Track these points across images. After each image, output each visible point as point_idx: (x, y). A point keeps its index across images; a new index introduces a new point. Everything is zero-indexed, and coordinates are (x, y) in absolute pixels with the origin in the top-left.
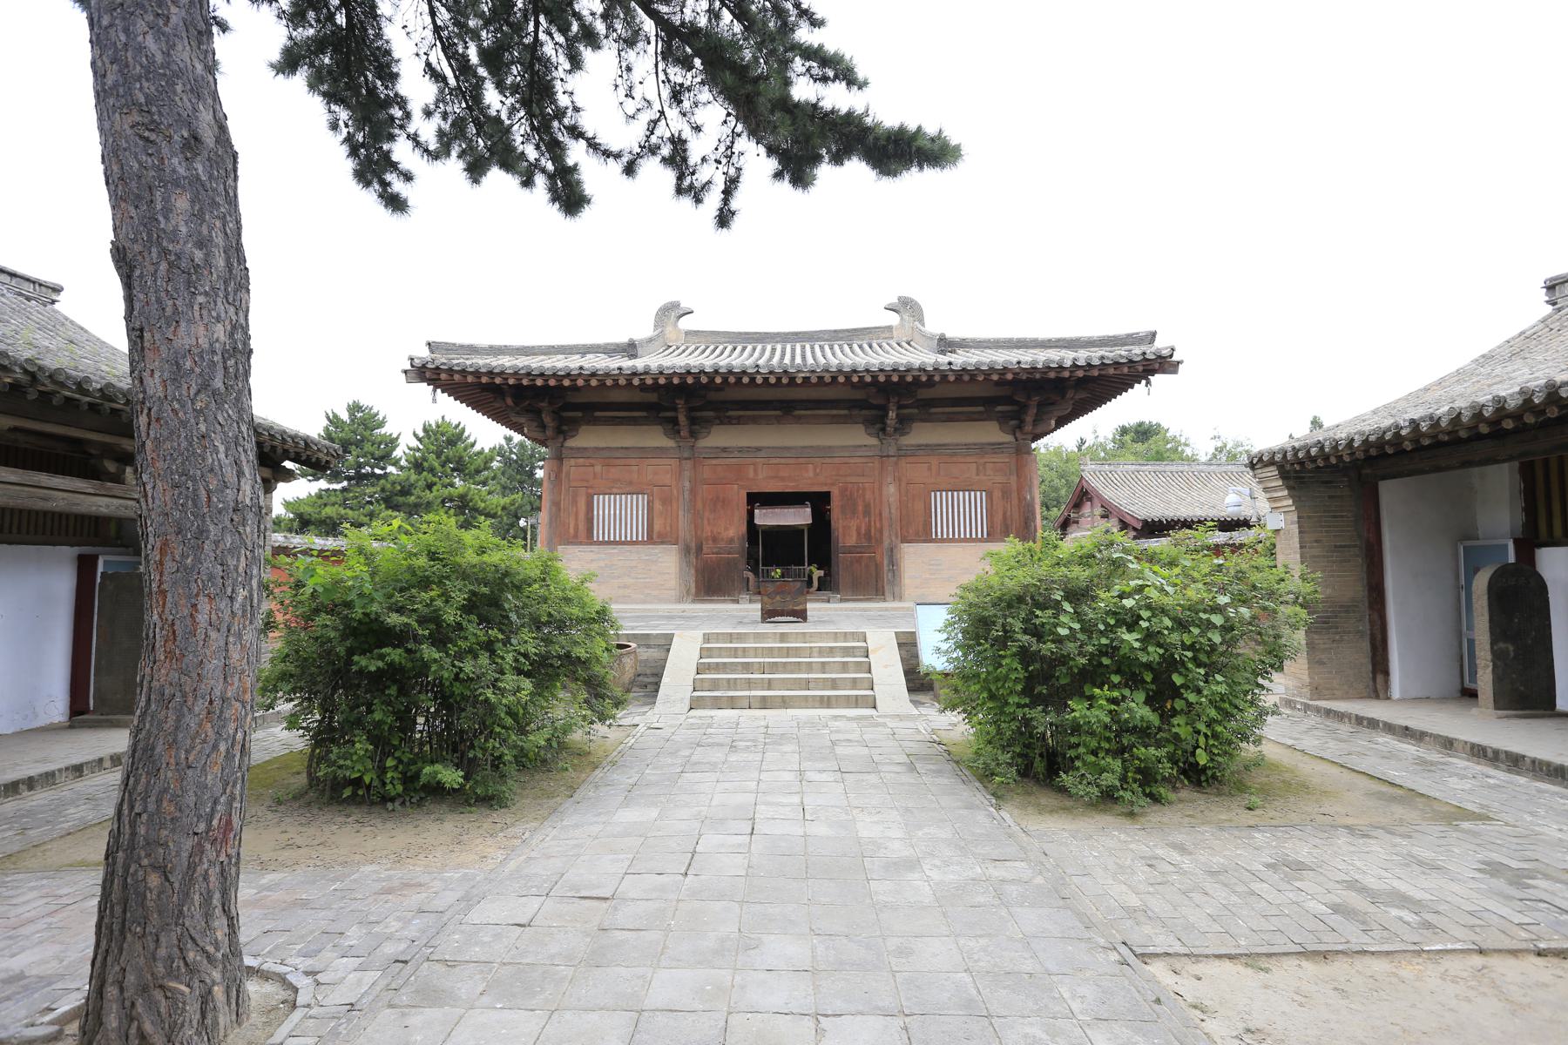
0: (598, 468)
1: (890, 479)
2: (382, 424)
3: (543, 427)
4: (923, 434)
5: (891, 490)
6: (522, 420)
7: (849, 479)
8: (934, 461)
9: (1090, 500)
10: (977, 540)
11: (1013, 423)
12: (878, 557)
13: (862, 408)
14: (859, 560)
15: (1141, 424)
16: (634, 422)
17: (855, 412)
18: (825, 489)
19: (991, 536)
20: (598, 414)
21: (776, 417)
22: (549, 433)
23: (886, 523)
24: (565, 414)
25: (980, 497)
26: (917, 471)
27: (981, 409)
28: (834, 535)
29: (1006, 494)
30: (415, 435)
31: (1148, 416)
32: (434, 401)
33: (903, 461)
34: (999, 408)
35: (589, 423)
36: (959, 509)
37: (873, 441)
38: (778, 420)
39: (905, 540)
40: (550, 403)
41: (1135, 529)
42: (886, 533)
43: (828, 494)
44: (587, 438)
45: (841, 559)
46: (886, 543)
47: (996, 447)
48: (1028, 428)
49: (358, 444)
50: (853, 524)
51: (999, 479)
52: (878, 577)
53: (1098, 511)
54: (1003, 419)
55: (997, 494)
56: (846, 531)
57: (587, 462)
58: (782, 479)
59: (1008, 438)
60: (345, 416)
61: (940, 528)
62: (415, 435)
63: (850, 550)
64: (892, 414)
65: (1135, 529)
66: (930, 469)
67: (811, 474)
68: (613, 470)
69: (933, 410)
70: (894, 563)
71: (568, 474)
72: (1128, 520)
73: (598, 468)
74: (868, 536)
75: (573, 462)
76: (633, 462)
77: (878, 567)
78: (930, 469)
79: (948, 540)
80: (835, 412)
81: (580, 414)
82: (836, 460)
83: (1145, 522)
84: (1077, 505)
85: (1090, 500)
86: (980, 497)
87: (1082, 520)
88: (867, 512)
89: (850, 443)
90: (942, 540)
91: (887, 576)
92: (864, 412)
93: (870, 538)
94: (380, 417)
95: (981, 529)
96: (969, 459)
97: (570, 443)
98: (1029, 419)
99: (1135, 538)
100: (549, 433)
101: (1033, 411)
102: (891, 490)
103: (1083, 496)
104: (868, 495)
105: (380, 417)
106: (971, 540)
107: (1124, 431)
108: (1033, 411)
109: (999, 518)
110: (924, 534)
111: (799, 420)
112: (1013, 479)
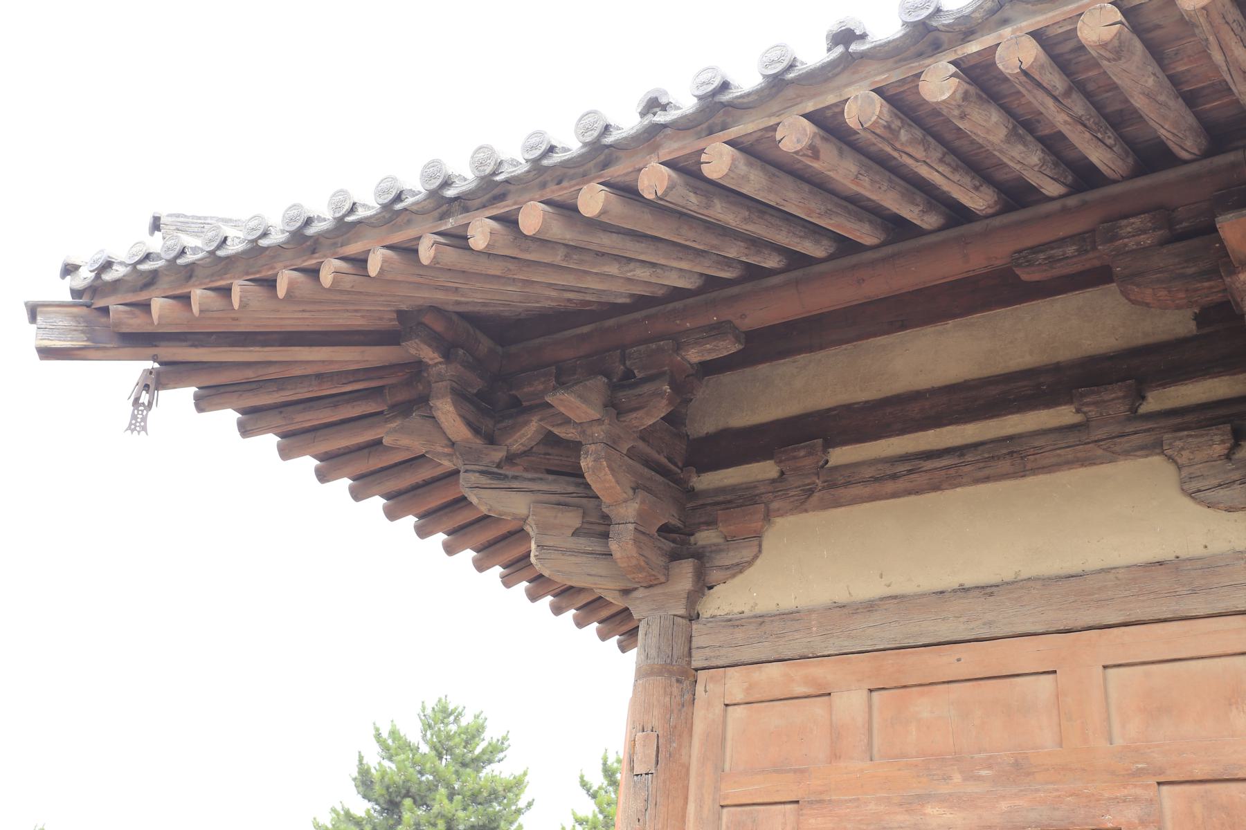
0: (850, 702)
2: (494, 752)
3: (599, 527)
6: (513, 504)
16: (1015, 459)
20: (841, 455)
22: (623, 545)
24: (708, 481)
30: (584, 784)
32: (138, 424)
35: (805, 500)
40: (615, 408)
44: (804, 566)
49: (421, 800)
57: (795, 677)
60: (413, 733)
62: (584, 784)
68: (924, 706)
71: (718, 741)
73: (850, 702)
75: (735, 683)
76: (1025, 654)
81: (765, 470)
94: (491, 734)
97: (727, 599)
100: (623, 545)
105: (491, 734)
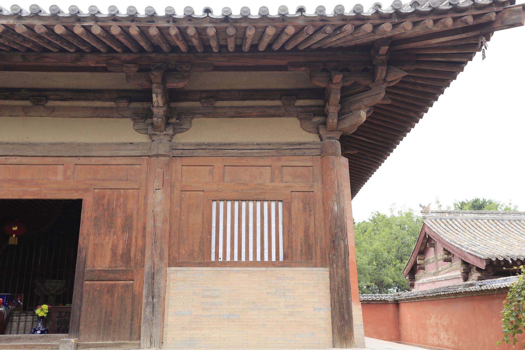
1: (157, 183)
4: (203, 131)
5: (158, 199)
7: (107, 184)
8: (218, 163)
9: (433, 245)
10: (270, 264)
11: (317, 119)
12: (137, 289)
13: (131, 100)
14: (111, 290)
15: (476, 201)
17: (123, 104)
18: (75, 196)
19: (289, 259)
21: (24, 108)
23: (149, 240)
25: (274, 210)
26: (196, 176)
27: (278, 103)
28: (80, 256)
29: (308, 205)
31: (482, 196)
33: (177, 164)
34: (300, 103)
36: (249, 223)
37: (142, 138)
38: (26, 112)
39: (174, 262)
41: (479, 269)
42: (148, 254)
43: (79, 203)
45: (86, 289)
46: (147, 269)
47: (296, 148)
48: (332, 120)
50: (108, 241)
51: (299, 186)
52: (135, 315)
53: (441, 254)
54: (304, 116)
55: (297, 206)
56: (96, 248)
58: (21, 183)
59: (312, 138)
61: (221, 246)
63: (100, 276)
64: (157, 99)
65: (479, 269)
66: (211, 173)
67: (60, 177)
69: (219, 104)
70: (156, 297)
72: (471, 260)
74: (126, 257)
77: (136, 299)
78: (211, 173)
79: (232, 264)
80: (98, 104)
82: (93, 160)
83: (489, 262)
84: (422, 252)
85: (433, 245)
86: (274, 210)
87: (427, 267)
88: (127, 226)
89: (115, 140)
90: (224, 264)
91: (146, 311)
92: (134, 105)
93: (128, 262)
95: (276, 248)
96: (261, 162)
98: (333, 109)
99: (480, 279)
101: (335, 97)
102: (158, 199)
103: (426, 242)
104: (131, 205)
106: (263, 264)
107: (463, 204)
108: (335, 97)
109: (299, 236)
110: (200, 256)
111: (52, 111)
112: (317, 187)
